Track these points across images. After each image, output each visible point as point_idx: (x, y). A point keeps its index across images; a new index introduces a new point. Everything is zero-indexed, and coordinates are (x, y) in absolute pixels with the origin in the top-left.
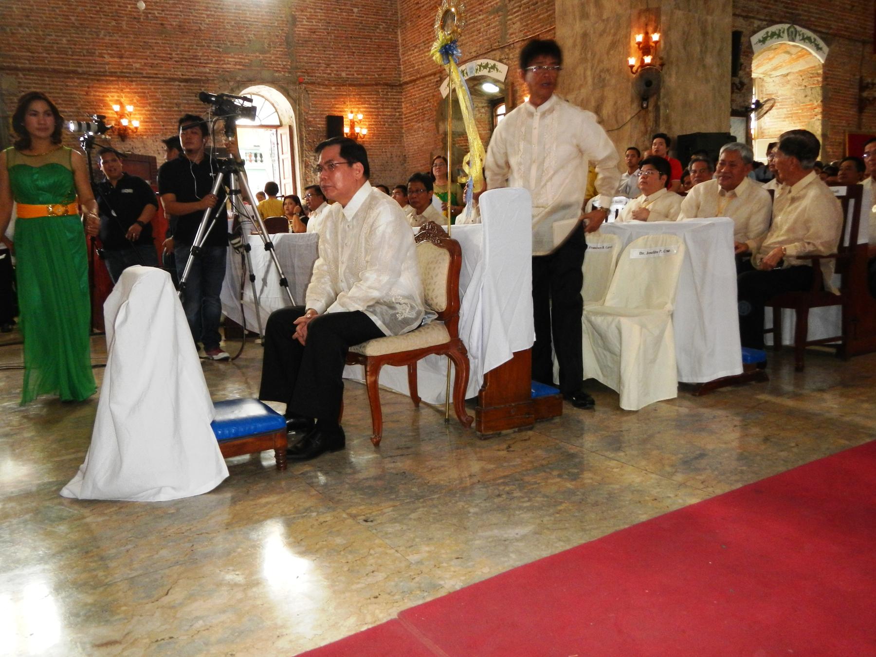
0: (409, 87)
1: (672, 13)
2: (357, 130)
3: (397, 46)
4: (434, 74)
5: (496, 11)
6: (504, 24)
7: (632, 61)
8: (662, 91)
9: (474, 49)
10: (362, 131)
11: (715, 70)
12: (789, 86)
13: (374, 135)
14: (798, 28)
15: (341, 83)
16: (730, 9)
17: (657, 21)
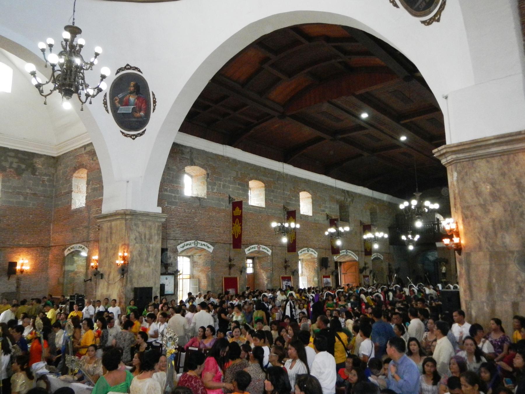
0: (53, 248)
1: (134, 245)
2: (24, 268)
3: (49, 231)
4: (63, 245)
5: (86, 227)
6: (88, 232)
7: (117, 262)
8: (129, 271)
9: (78, 239)
10: (27, 268)
11: (153, 263)
12: (201, 260)
13: (33, 269)
14: (199, 241)
15: (19, 246)
16: (160, 241)
17: (128, 248)
